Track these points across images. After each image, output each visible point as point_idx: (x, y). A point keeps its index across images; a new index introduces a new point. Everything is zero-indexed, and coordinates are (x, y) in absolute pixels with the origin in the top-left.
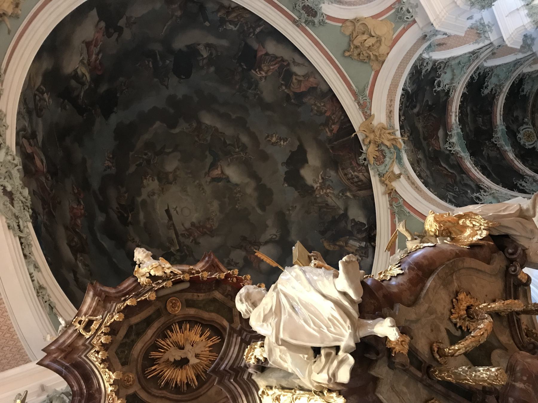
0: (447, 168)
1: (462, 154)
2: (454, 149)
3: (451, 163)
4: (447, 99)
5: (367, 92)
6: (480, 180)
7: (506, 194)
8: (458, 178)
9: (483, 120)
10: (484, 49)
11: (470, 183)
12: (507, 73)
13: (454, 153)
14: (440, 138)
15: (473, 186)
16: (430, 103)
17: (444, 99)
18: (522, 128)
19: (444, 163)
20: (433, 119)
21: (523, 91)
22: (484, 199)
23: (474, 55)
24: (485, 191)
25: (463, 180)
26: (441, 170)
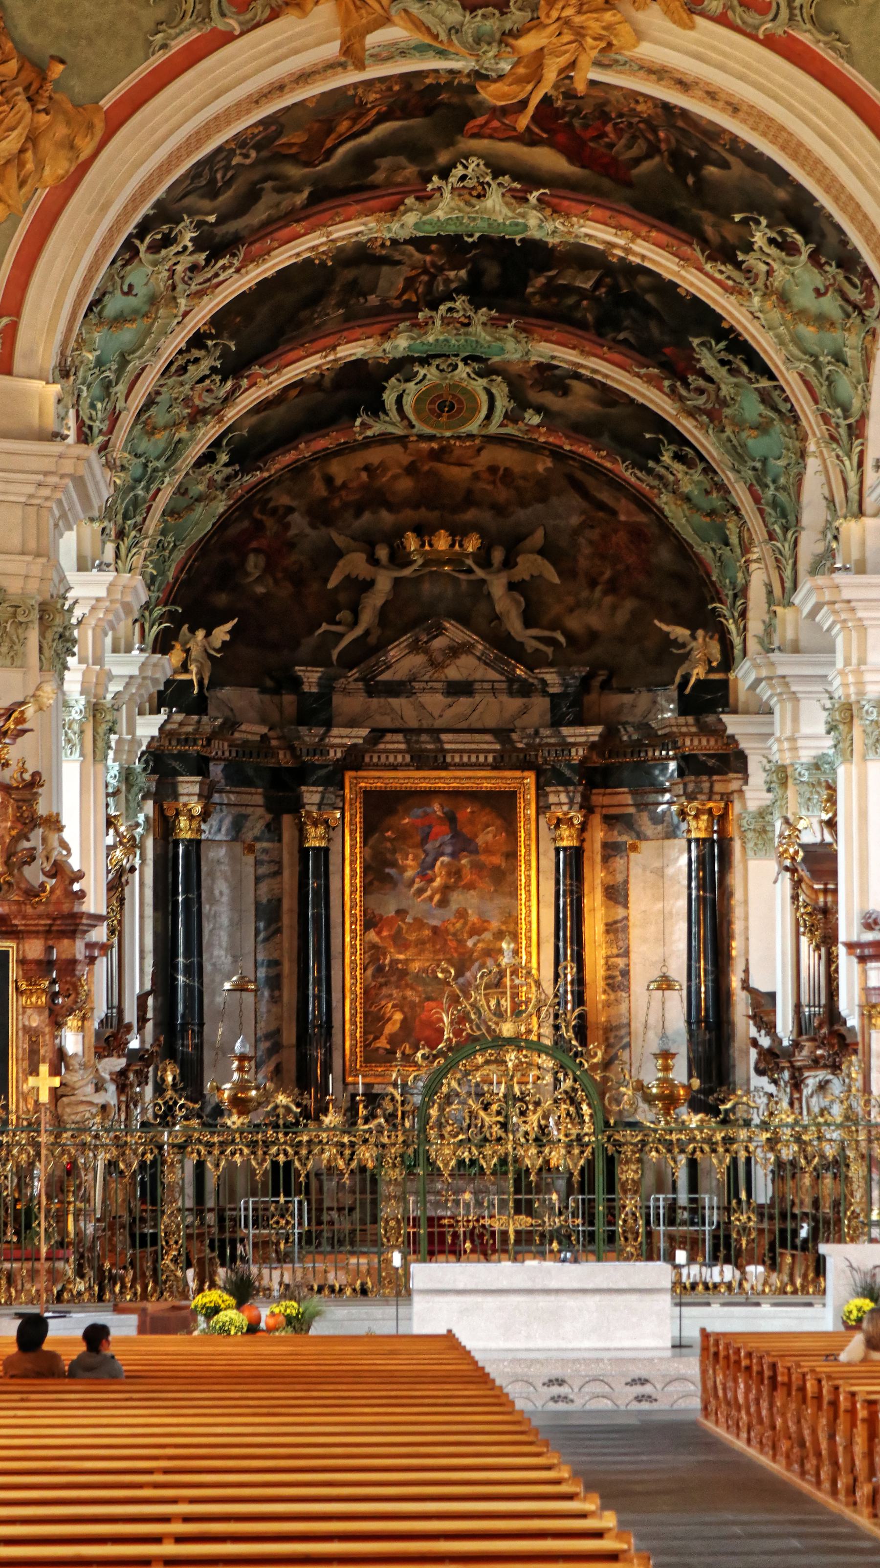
0: (365, 139)
1: (411, 219)
2: (447, 191)
3: (384, 163)
4: (704, 242)
5: (806, 37)
6: (251, 259)
7: (156, 351)
8: (294, 172)
9: (580, 291)
10: (852, 478)
11: (259, 214)
12: (758, 465)
13: (430, 187)
14: (526, 149)
15: (234, 226)
16: (711, 171)
17: (709, 231)
18: (501, 391)
19: (394, 133)
20: (634, 152)
21: (678, 457)
22: (155, 264)
23: (843, 431)
24: (194, 268)
25: (279, 190)
26: (361, 115)
